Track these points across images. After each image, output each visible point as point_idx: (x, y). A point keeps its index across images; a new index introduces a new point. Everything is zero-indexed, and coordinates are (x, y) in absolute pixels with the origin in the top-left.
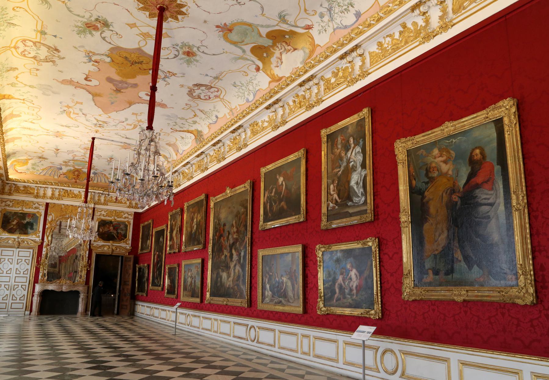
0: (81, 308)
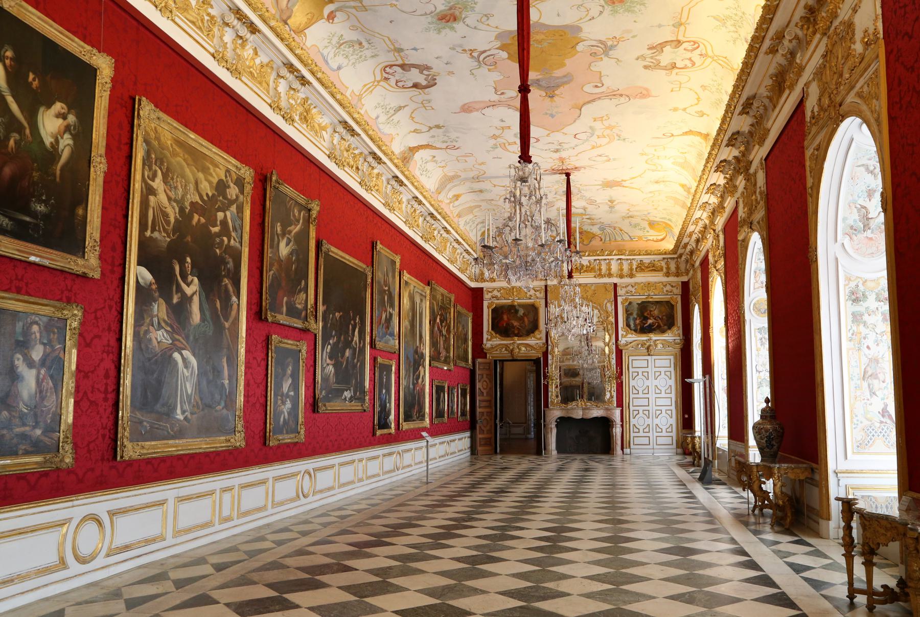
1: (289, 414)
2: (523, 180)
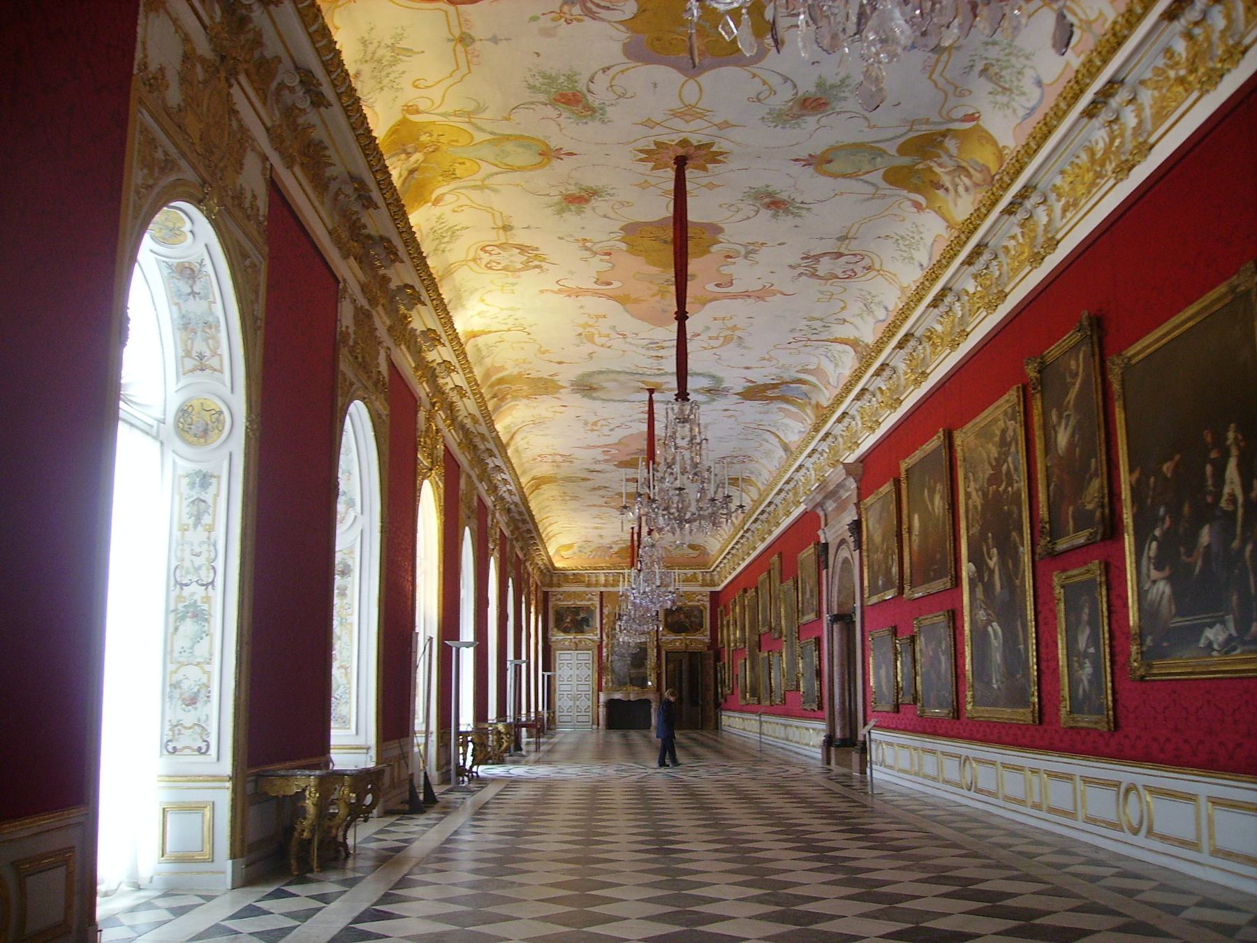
1: (1090, 682)
2: (684, 420)
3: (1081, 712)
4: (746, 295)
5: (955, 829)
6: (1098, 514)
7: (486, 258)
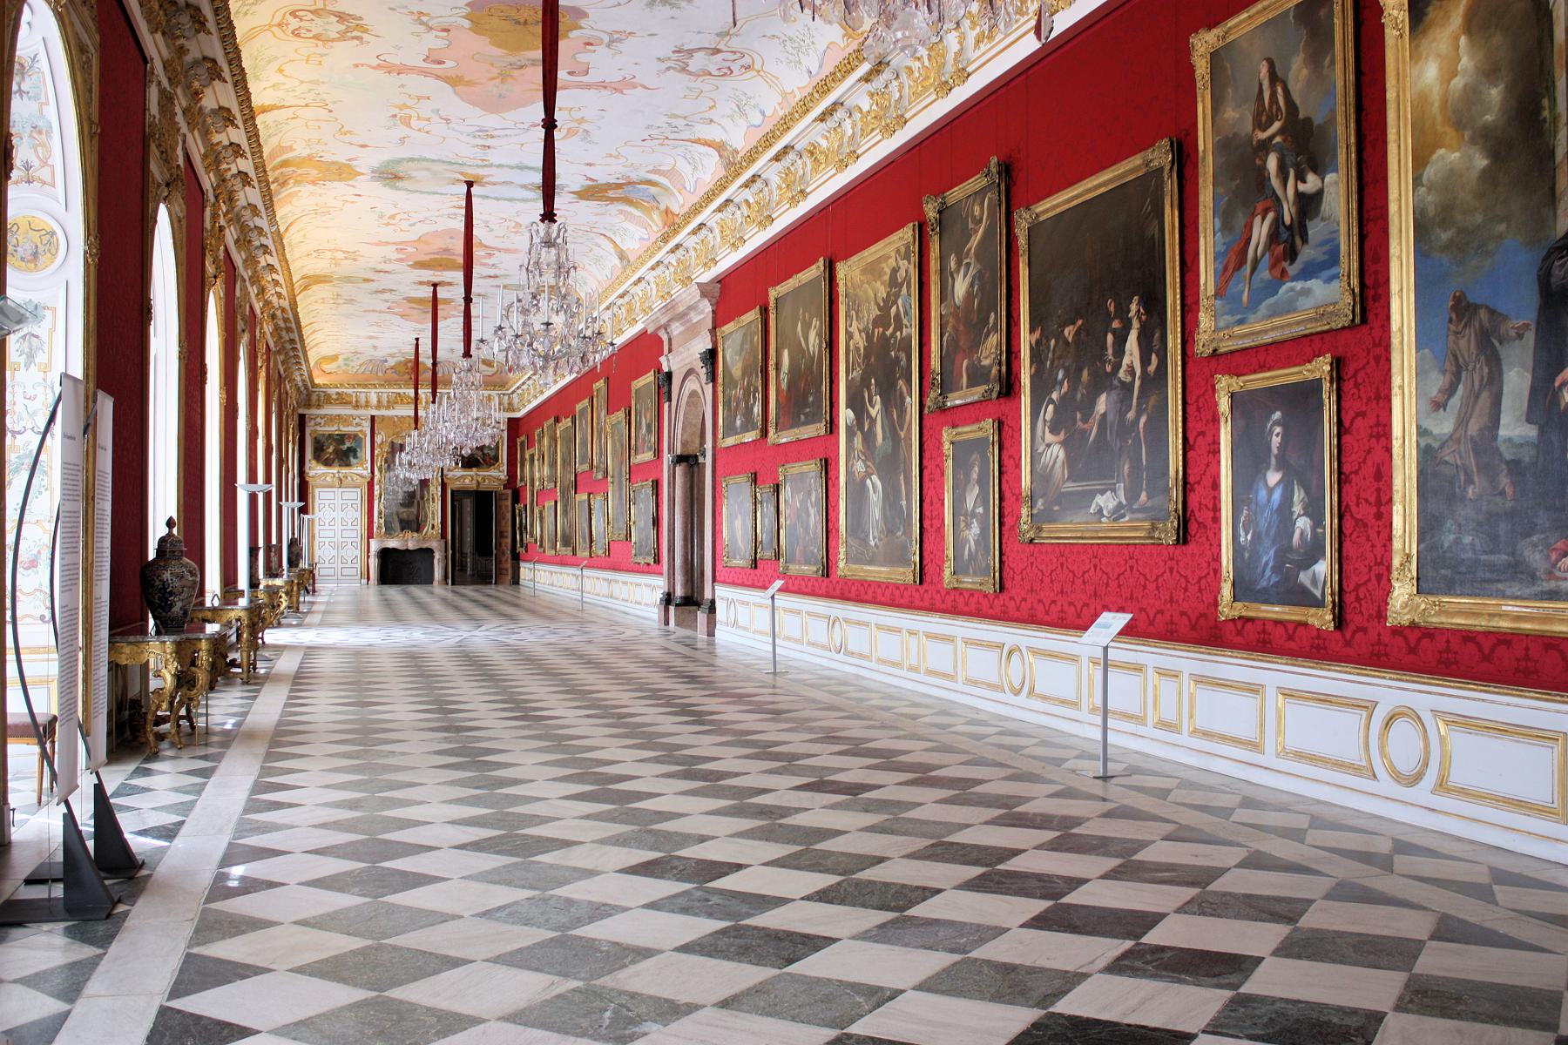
0: (438, 573)
1: (976, 542)
3: (967, 574)
4: (603, 86)
5: (829, 692)
6: (994, 371)
7: (294, 23)
